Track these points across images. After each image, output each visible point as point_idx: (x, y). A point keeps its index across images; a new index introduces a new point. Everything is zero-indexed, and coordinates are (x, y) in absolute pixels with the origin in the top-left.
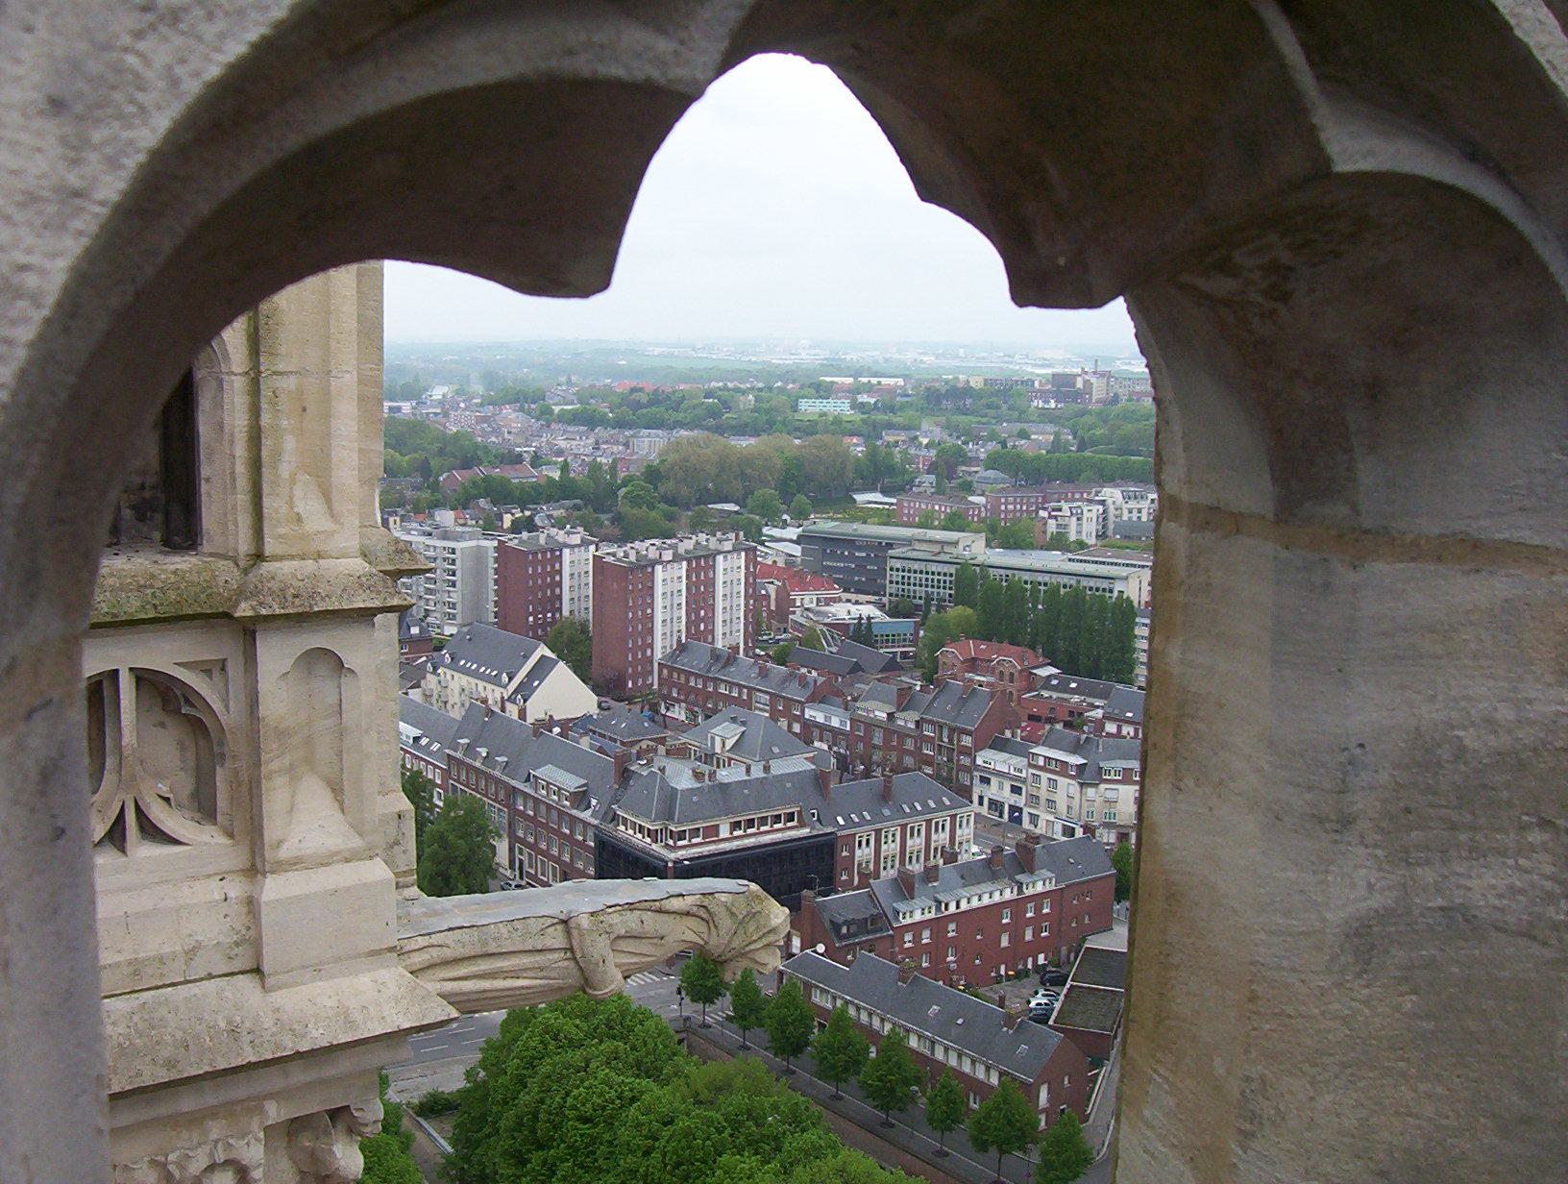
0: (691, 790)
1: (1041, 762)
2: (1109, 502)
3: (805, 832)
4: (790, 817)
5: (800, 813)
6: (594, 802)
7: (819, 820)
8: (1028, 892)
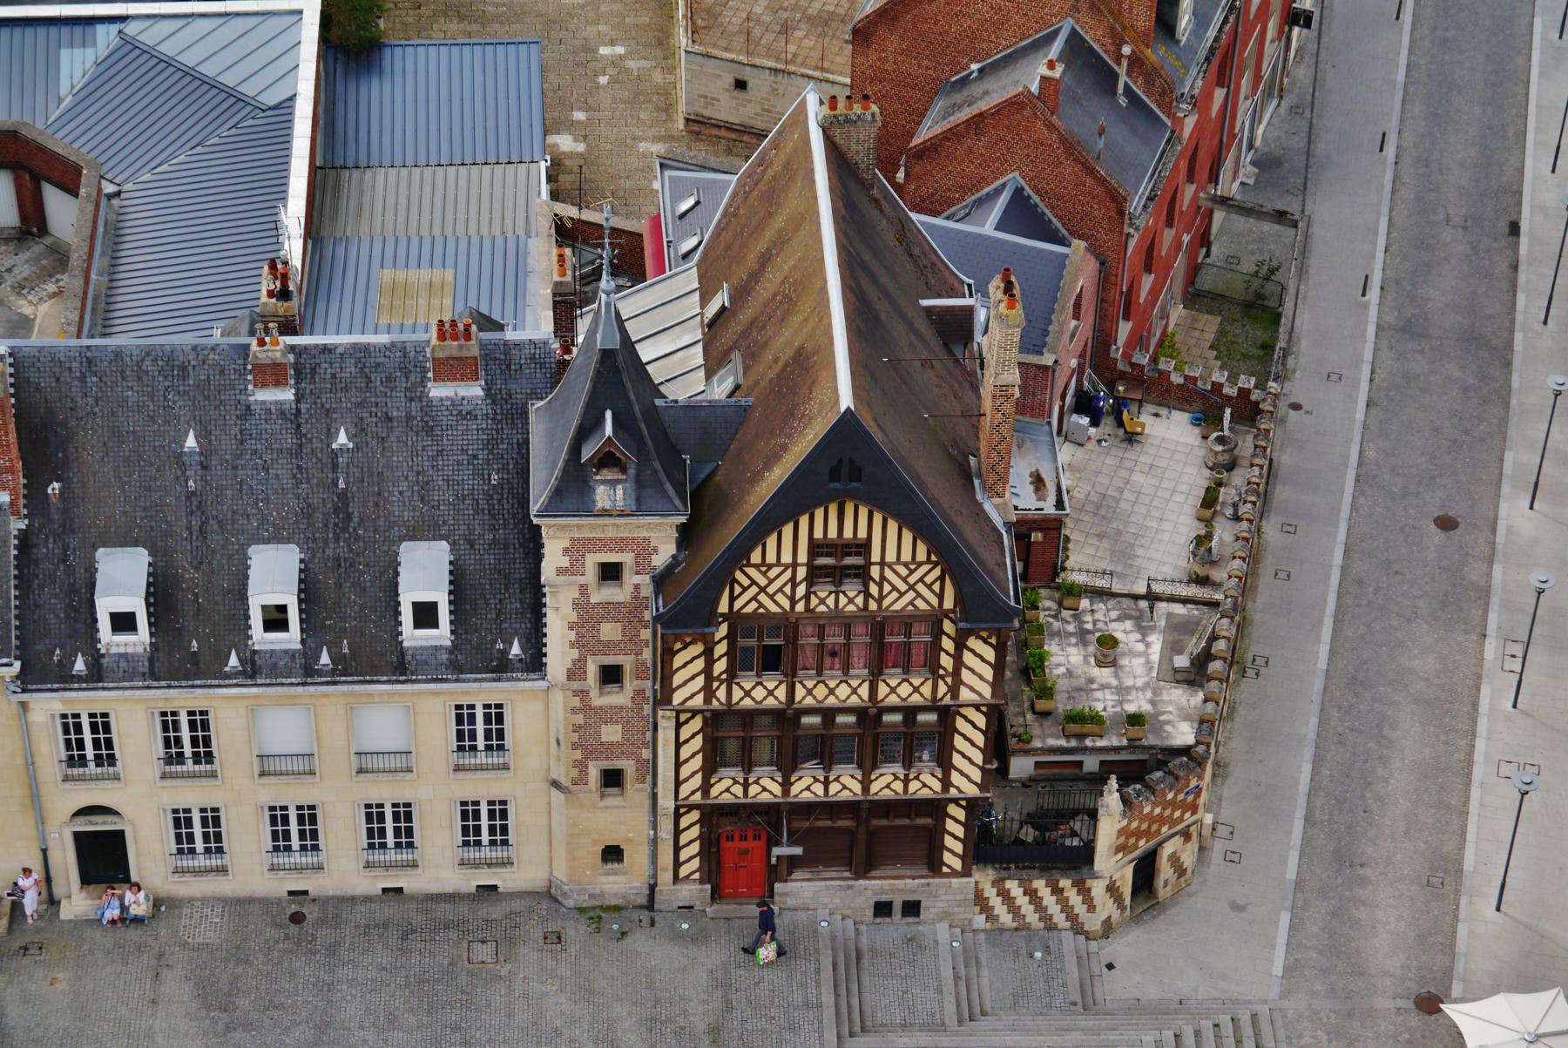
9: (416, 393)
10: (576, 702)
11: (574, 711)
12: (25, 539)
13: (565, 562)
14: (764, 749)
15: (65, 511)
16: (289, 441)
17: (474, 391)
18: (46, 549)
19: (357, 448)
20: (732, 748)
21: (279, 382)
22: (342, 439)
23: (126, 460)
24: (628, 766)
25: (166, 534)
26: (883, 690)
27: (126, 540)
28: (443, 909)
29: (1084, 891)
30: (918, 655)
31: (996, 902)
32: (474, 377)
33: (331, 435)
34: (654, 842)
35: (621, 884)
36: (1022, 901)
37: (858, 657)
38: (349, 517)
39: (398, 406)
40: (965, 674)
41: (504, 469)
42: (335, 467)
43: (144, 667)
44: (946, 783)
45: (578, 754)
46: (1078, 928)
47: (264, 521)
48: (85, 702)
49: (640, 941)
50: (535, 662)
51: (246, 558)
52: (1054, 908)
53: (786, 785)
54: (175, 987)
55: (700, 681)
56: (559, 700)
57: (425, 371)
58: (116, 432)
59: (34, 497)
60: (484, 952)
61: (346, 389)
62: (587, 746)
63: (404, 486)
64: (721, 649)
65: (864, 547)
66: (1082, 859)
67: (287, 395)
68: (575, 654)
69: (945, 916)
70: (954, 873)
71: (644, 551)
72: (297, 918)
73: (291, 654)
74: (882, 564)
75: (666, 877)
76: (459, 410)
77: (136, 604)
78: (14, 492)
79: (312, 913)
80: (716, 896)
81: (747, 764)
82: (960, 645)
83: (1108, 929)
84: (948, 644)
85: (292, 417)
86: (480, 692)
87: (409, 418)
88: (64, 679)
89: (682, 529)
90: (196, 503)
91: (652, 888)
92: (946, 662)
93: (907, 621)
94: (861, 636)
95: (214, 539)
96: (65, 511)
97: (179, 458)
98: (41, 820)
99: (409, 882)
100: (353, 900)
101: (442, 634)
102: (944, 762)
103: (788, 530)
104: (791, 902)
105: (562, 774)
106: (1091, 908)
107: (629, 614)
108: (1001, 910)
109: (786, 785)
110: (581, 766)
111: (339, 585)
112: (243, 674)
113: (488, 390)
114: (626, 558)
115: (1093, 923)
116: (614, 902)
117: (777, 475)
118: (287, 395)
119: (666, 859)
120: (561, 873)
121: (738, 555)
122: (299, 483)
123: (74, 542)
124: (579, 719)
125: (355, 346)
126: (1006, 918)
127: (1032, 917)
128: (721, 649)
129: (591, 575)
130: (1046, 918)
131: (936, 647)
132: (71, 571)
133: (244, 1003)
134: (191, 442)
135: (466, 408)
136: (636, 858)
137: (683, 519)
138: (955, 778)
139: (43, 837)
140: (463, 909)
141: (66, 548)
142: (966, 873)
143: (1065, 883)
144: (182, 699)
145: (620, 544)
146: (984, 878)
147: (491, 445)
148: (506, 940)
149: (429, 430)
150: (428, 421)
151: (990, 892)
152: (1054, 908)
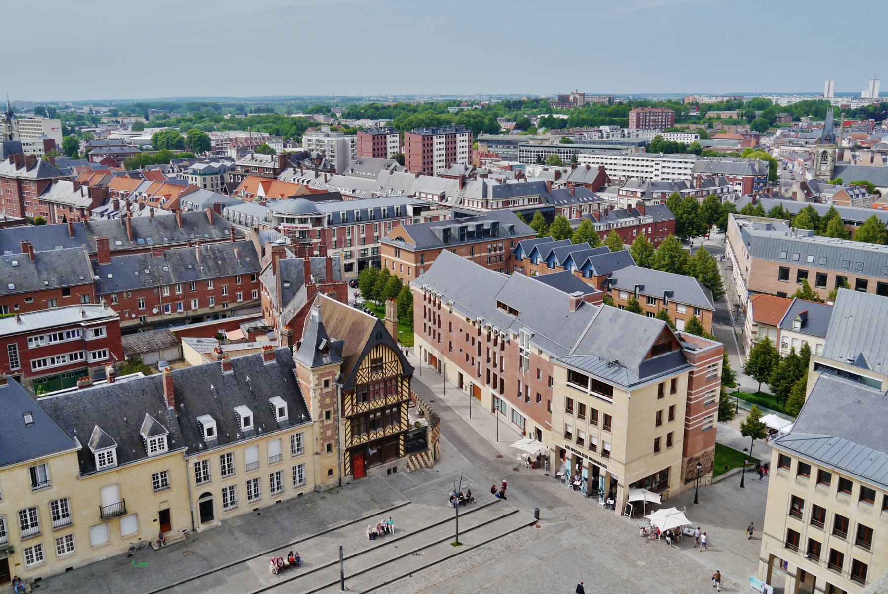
0: (497, 186)
1: (624, 193)
2: (604, 132)
3: (542, 205)
4: (535, 200)
5: (539, 198)
6: (449, 199)
7: (547, 202)
8: (643, 223)
9: (261, 364)
10: (321, 425)
11: (321, 428)
12: (179, 419)
13: (317, 382)
14: (362, 429)
15: (186, 410)
16: (236, 382)
17: (274, 362)
20: (356, 429)
21: (230, 369)
22: (248, 378)
24: (333, 442)
25: (213, 410)
26: (388, 400)
28: (292, 502)
29: (427, 455)
30: (393, 387)
31: (410, 463)
33: (245, 378)
34: (340, 465)
35: (333, 481)
36: (416, 461)
37: (382, 392)
39: (258, 369)
40: (403, 392)
42: (248, 385)
43: (217, 443)
44: (400, 427)
45: (322, 441)
46: (427, 466)
47: (235, 402)
49: (343, 492)
50: (308, 418)
52: (422, 462)
53: (368, 437)
54: (237, 534)
55: (351, 407)
56: (317, 426)
59: (177, 408)
60: (309, 505)
62: (324, 438)
64: (355, 396)
65: (381, 359)
66: (424, 447)
67: (232, 372)
68: (320, 410)
69: (402, 469)
70: (403, 456)
71: (334, 375)
72: (259, 514)
73: (252, 430)
74: (386, 363)
75: (343, 475)
79: (262, 512)
80: (354, 479)
81: (359, 433)
82: (402, 384)
83: (432, 467)
84: (399, 384)
85: (235, 376)
86: (296, 429)
88: (198, 450)
89: (342, 366)
90: (218, 401)
91: (340, 479)
92: (399, 389)
93: (390, 379)
94: (382, 385)
95: (225, 408)
96: (186, 410)
97: (210, 392)
99: (283, 498)
100: (270, 507)
101: (286, 417)
102: (399, 422)
103: (366, 358)
104: (370, 475)
105: (318, 449)
106: (429, 460)
107: (332, 395)
108: (412, 466)
109: (368, 437)
110: (322, 445)
113: (277, 361)
114: (330, 377)
115: (430, 465)
116: (331, 487)
117: (363, 343)
119: (343, 470)
120: (318, 483)
121: (356, 370)
124: (322, 430)
126: (413, 468)
127: (418, 466)
128: (355, 396)
129: (323, 385)
130: (421, 465)
131: (397, 385)
132: (192, 424)
133: (259, 531)
134: (212, 387)
136: (336, 472)
137: (342, 362)
138: (402, 425)
139: (191, 508)
140: (298, 500)
141: (189, 419)
142: (404, 456)
143: (423, 454)
144: (226, 449)
145: (328, 374)
146: (408, 456)
147: (282, 373)
148: (313, 501)
150: (266, 370)
151: (409, 461)
152: (422, 462)
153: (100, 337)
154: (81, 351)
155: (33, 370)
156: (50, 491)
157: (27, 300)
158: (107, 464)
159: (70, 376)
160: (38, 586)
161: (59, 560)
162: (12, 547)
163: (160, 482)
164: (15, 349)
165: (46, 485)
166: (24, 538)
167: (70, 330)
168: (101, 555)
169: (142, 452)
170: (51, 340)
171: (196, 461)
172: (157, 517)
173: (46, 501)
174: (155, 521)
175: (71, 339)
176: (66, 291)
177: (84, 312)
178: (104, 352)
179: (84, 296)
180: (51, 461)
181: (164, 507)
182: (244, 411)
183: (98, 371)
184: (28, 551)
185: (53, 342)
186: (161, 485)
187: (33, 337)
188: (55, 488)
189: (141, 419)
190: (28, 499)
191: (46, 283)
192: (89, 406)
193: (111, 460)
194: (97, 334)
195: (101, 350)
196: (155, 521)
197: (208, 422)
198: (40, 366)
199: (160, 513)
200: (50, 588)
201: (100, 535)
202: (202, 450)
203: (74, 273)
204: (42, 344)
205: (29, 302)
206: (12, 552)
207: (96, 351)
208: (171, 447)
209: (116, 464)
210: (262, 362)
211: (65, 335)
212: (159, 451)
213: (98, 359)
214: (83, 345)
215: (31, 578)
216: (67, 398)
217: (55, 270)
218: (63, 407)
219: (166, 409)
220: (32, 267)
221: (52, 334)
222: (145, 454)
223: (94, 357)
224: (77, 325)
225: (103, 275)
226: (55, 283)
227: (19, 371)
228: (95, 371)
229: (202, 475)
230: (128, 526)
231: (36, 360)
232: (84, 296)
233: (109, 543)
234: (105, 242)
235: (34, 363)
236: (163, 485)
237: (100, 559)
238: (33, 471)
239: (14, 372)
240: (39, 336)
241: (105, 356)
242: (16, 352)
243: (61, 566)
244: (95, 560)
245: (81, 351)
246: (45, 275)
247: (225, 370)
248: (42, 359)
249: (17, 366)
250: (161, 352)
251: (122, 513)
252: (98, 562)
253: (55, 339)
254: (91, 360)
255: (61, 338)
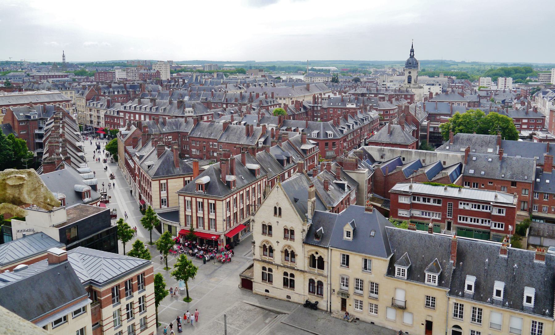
9: (531, 261)
12: (454, 271)
15: (463, 267)
16: (505, 264)
17: (543, 263)
18: (458, 273)
19: (518, 268)
22: (516, 265)
23: (475, 261)
25: (480, 275)
27: (472, 274)
32: (543, 260)
33: (513, 265)
38: (515, 280)
39: (527, 262)
41: (548, 278)
42: (514, 270)
43: (472, 297)
47: (498, 277)
48: (460, 301)
51: (494, 282)
57: (533, 257)
58: (474, 256)
59: (457, 264)
61: (518, 258)
63: (527, 276)
67: (506, 256)
73: (501, 302)
76: (540, 266)
77: (473, 284)
78: (454, 261)
85: (507, 261)
87: (529, 265)
88: (457, 295)
95: (489, 277)
96: (463, 267)
97: (484, 263)
98: (447, 326)
101: (532, 305)
111: (512, 291)
112: (491, 303)
113: (546, 263)
118: (506, 256)
122: (506, 272)
123: (463, 273)
125: (520, 251)
132: (461, 277)
134: (487, 260)
135: (541, 265)
141: (461, 273)
144: (478, 305)
147: (546, 273)
149: (533, 268)
150: (533, 266)
153: (501, 215)
154: (489, 220)
155: (459, 221)
156: (371, 276)
157: (489, 183)
158: (401, 276)
159: (479, 232)
160: (355, 322)
161: (369, 315)
162: (349, 295)
163: (430, 302)
164: (452, 206)
165: (369, 271)
166: (355, 293)
167: (485, 205)
168: (390, 326)
169: (422, 279)
170: (472, 208)
171: (455, 301)
172: (425, 323)
173: (368, 280)
174: (423, 324)
175: (485, 210)
176: (514, 184)
177: (496, 197)
178: (502, 225)
179: (525, 189)
180: (373, 259)
181: (429, 319)
182: (499, 286)
183: (496, 235)
184: (356, 301)
185: (473, 209)
186: (430, 305)
187: (463, 202)
188: (373, 275)
189: (431, 260)
190: (361, 275)
191: (503, 176)
192: (408, 240)
193: (403, 275)
194: (499, 212)
195: (501, 223)
196: (423, 324)
197: (470, 280)
198: (463, 220)
199: (427, 321)
200: (358, 326)
201: (392, 314)
202: (460, 296)
203: (523, 174)
204: (467, 208)
205: (490, 184)
206: (348, 297)
207: (497, 223)
208: (440, 284)
209: (406, 278)
210: (533, 259)
211: (481, 207)
212: (432, 283)
213: (497, 228)
214: (489, 216)
215: (355, 316)
216: (400, 231)
217: (512, 169)
218: (395, 235)
219: (449, 261)
220: (498, 164)
221: (474, 204)
222: (424, 281)
223: (495, 226)
224: (488, 203)
225: (543, 180)
226: (509, 177)
227: (451, 219)
228: (493, 235)
229: (459, 312)
230: (407, 318)
231: (462, 216)
232: (525, 189)
233: (395, 322)
234: (550, 158)
235: (460, 218)
236: (432, 306)
237: (389, 327)
238: (366, 261)
239: (448, 219)
240: (466, 203)
241: (502, 227)
242: (451, 208)
243: (369, 319)
244: (387, 327)
245: (489, 220)
246: (504, 171)
247: (501, 253)
248: (465, 216)
249: (451, 216)
250: (542, 238)
251: (403, 308)
252: (387, 328)
253: (475, 208)
254: (493, 227)
255: (479, 208)
